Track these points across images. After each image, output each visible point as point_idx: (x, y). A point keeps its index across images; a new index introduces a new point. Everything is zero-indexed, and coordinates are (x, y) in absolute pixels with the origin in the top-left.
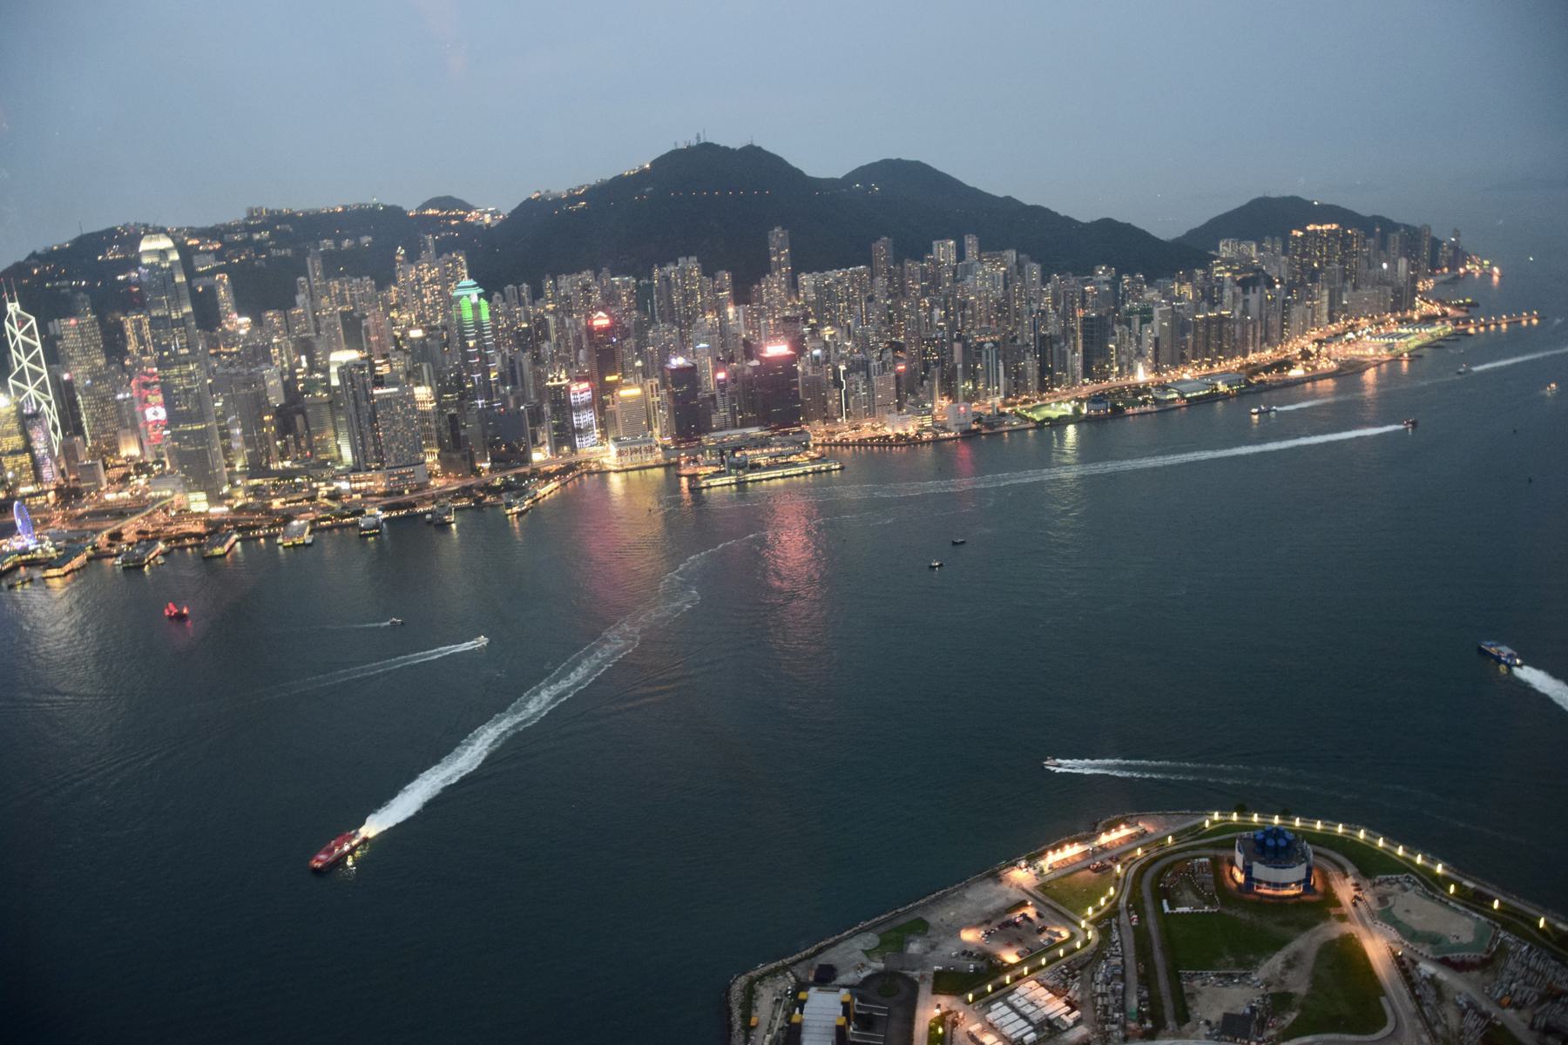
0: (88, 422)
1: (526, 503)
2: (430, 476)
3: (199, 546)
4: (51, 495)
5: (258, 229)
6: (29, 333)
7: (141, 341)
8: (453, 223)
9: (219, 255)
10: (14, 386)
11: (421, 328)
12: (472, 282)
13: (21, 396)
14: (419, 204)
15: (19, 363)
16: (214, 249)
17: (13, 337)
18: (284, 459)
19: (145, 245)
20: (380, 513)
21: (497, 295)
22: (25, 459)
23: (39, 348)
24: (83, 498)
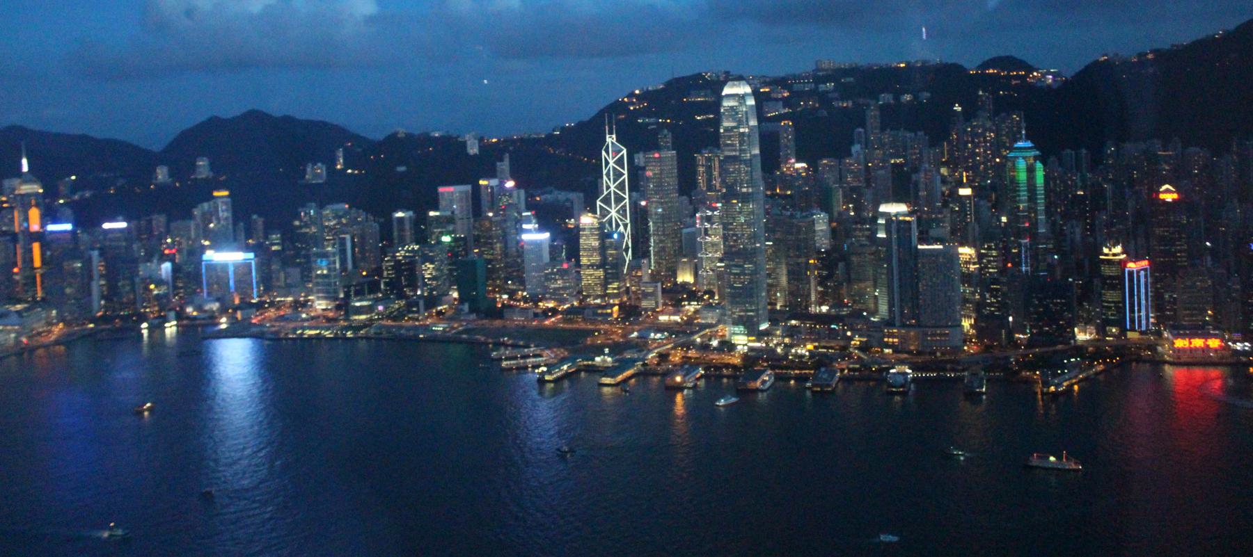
0: (654, 247)
1: (1065, 384)
2: (965, 342)
3: (735, 377)
4: (616, 308)
5: (825, 79)
6: (620, 162)
7: (709, 180)
8: (1014, 82)
9: (786, 102)
10: (600, 206)
11: (970, 187)
12: (1029, 144)
13: (603, 216)
14: (979, 62)
15: (608, 187)
16: (783, 96)
17: (607, 163)
18: (821, 304)
19: (727, 91)
20: (910, 371)
21: (1052, 159)
22: (600, 273)
23: (626, 176)
24: (641, 315)
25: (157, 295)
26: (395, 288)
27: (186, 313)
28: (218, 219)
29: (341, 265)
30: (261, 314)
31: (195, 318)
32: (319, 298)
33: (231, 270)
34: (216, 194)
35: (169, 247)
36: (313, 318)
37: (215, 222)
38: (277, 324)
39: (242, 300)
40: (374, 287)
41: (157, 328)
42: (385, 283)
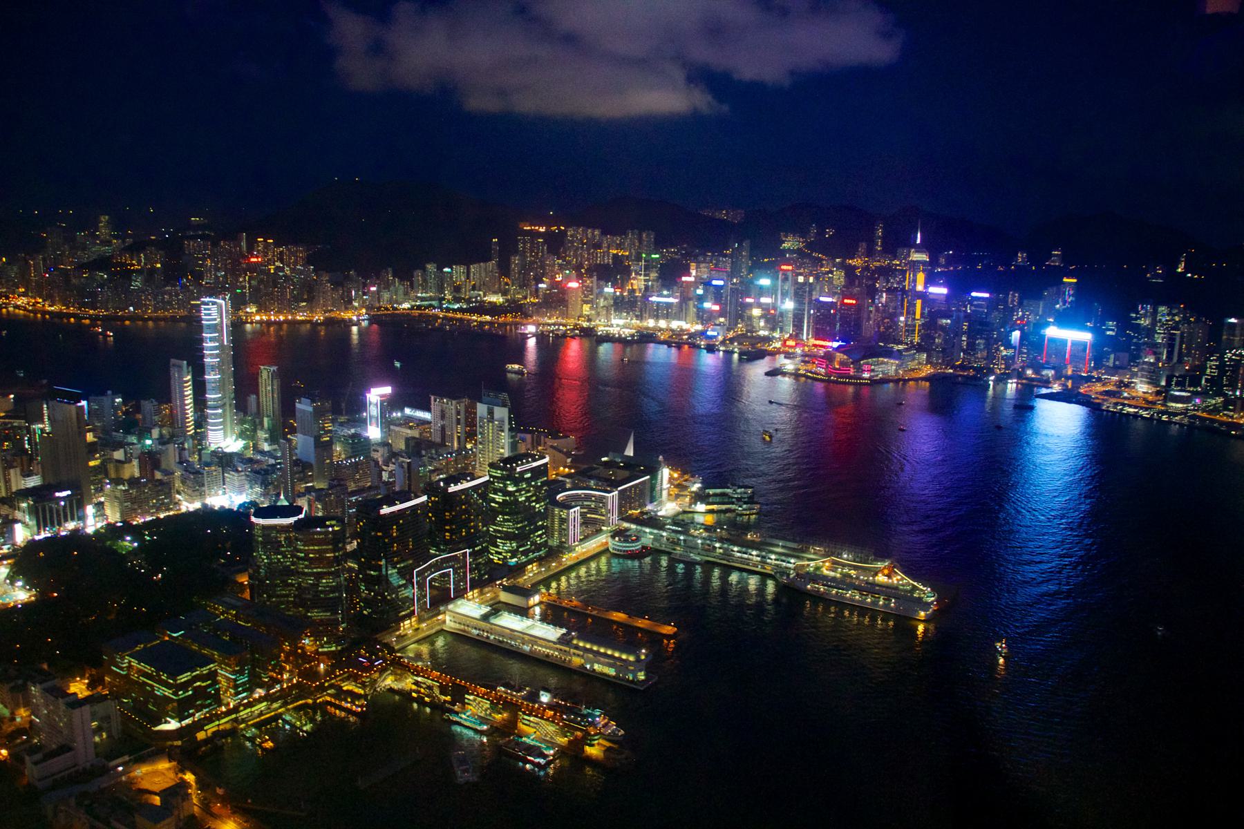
25: (1006, 355)
26: (1216, 386)
27: (1025, 374)
28: (1064, 305)
29: (1167, 357)
30: (1088, 387)
31: (1032, 380)
32: (1141, 381)
33: (1069, 344)
34: (1065, 280)
35: (1022, 319)
36: (1134, 398)
37: (1061, 304)
38: (1102, 397)
39: (1073, 371)
40: (1195, 381)
41: (1002, 379)
42: (1206, 379)
